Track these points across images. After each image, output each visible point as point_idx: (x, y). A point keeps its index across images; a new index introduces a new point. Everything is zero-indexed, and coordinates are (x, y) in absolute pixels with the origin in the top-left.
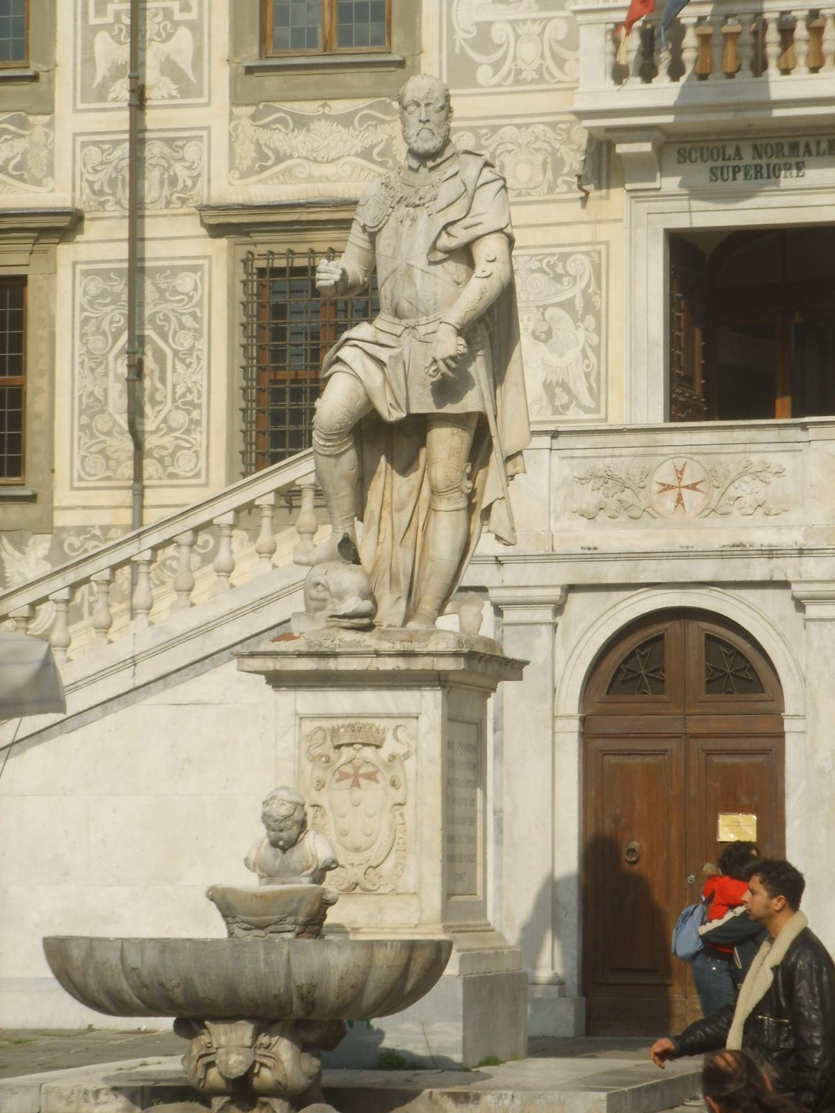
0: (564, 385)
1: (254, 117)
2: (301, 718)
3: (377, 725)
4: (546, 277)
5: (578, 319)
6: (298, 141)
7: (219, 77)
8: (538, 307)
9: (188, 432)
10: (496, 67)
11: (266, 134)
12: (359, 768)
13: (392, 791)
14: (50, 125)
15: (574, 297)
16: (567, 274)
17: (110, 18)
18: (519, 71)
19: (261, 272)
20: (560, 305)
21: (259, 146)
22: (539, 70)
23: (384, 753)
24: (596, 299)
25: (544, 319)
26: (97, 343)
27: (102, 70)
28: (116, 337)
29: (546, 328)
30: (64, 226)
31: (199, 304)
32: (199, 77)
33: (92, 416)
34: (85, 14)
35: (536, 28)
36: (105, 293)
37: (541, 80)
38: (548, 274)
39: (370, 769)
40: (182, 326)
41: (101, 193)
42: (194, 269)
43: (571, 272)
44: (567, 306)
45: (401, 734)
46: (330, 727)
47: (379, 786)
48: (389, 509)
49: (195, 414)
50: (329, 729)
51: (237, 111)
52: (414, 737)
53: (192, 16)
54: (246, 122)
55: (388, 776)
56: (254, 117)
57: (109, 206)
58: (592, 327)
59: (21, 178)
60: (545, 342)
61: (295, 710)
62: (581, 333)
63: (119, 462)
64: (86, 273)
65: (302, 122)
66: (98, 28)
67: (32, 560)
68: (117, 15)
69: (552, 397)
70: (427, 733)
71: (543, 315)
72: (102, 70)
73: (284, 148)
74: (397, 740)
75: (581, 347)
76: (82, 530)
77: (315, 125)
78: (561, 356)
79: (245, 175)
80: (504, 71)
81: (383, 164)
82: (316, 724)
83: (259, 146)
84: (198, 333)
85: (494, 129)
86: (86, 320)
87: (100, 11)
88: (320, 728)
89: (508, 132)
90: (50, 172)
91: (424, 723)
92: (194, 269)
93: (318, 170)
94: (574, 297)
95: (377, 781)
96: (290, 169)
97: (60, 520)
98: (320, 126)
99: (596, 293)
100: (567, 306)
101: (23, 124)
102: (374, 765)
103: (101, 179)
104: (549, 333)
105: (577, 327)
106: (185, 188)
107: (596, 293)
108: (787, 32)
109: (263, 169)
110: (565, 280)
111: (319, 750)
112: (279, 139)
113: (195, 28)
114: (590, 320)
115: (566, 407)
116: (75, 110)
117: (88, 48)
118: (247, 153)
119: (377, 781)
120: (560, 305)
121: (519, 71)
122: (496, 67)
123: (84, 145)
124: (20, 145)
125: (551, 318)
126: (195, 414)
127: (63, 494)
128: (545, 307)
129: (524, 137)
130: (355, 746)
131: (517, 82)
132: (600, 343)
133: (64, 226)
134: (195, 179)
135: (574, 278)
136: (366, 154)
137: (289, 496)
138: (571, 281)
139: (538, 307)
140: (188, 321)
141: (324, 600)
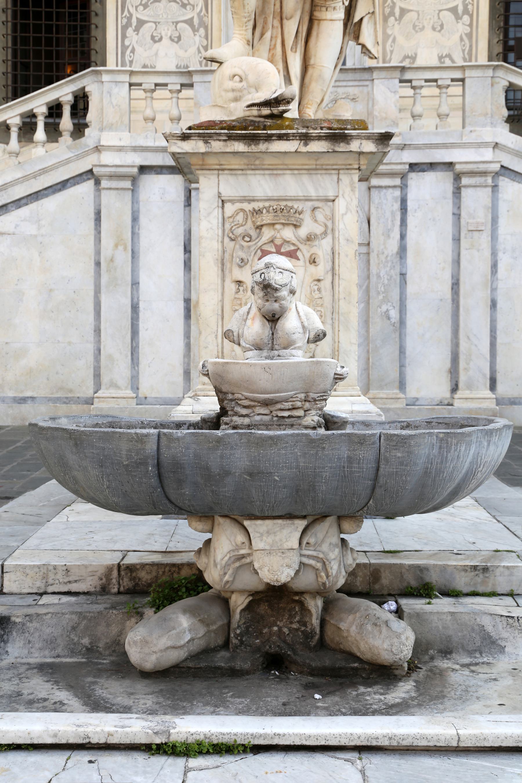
2: (222, 201)
3: (296, 206)
4: (177, 5)
5: (195, 30)
8: (173, 23)
12: (281, 245)
13: (312, 268)
15: (193, 18)
16: (189, 4)
20: (185, 22)
23: (303, 232)
24: (205, 19)
25: (176, 30)
29: (177, 35)
38: (178, 3)
39: (292, 248)
43: (192, 2)
44: (190, 22)
45: (320, 216)
46: (251, 209)
47: (301, 263)
48: (279, 18)
50: (250, 211)
52: (332, 218)
55: (307, 256)
58: (203, 35)
60: (177, 42)
61: (219, 193)
62: (197, 38)
70: (346, 214)
71: (176, 27)
74: (316, 221)
75: (197, 46)
78: (186, 51)
82: (238, 205)
88: (242, 210)
91: (341, 205)
94: (193, 18)
95: (298, 259)
99: (205, 16)
100: (190, 22)
102: (294, 244)
104: (179, 38)
105: (195, 35)
107: (205, 16)
110: (188, 7)
111: (240, 231)
119: (298, 259)
120: (185, 22)
125: (180, 29)
128: (177, 23)
130: (277, 227)
132: (207, 45)
135: (193, 6)
138: (191, 7)
139: (173, 23)
141: (240, 90)
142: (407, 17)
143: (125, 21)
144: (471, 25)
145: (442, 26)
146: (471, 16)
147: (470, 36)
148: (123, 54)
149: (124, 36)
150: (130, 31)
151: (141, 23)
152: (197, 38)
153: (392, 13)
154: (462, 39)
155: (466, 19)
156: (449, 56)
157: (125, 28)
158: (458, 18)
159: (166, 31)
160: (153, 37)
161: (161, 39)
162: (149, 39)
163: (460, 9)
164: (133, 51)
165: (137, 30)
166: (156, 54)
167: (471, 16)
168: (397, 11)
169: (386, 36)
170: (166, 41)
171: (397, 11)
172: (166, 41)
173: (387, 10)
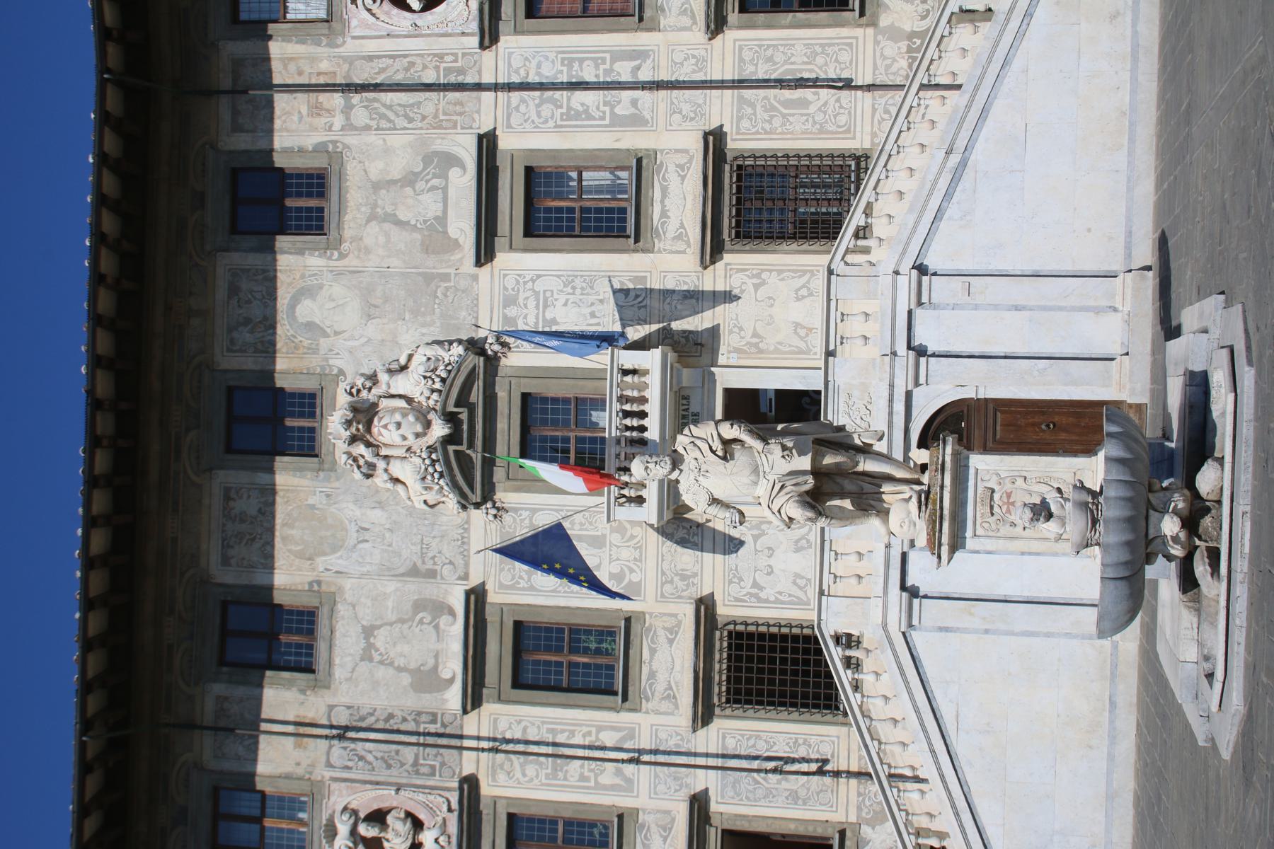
0: (797, 542)
1: (648, 700)
5: (763, 534)
6: (662, 677)
7: (625, 718)
9: (810, 746)
10: (632, 571)
11: (656, 694)
14: (644, 811)
17: (592, 775)
18: (635, 559)
19: (728, 701)
21: (663, 699)
22: (636, 549)
26: (760, 793)
27: (618, 781)
28: (757, 782)
30: (699, 805)
31: (742, 736)
32: (625, 728)
33: (798, 798)
34: (588, 788)
35: (614, 549)
36: (734, 787)
37: (640, 547)
40: (754, 746)
41: (681, 786)
42: (724, 738)
49: (801, 741)
51: (644, 709)
53: (594, 730)
54: (650, 705)
56: (648, 700)
57: (689, 781)
59: (671, 829)
62: (771, 532)
63: (824, 785)
64: (723, 797)
65: (652, 675)
66: (596, 782)
67: (874, 836)
68: (591, 770)
69: (802, 549)
72: (618, 781)
73: (665, 685)
76: (859, 808)
77: (654, 668)
79: (677, 707)
80: (635, 567)
81: (677, 633)
83: (663, 699)
84: (758, 737)
85: (663, 573)
86: (747, 798)
87: (586, 779)
89: (666, 566)
90: (668, 812)
92: (724, 738)
93: (677, 667)
96: (676, 683)
97: (853, 818)
98: (655, 666)
101: (643, 826)
103: (674, 786)
104: (769, 549)
106: (682, 740)
108: (627, 414)
109: (674, 697)
112: (660, 687)
113: (600, 729)
114: (764, 527)
115: (808, 541)
116: (637, 796)
117: (605, 787)
118: (665, 706)
121: (635, 559)
122: (632, 571)
123: (656, 793)
124: (654, 828)
126: (801, 741)
127: (838, 817)
129: (668, 557)
131: (640, 561)
133: (699, 805)
134: (678, 734)
136: (671, 642)
137: (848, 662)
140: (751, 742)
142: (760, 331)
143: (753, 599)
144: (770, 271)
145: (770, 298)
146: (763, 271)
147: (780, 272)
148: (782, 603)
149: (767, 601)
150: (763, 595)
151: (755, 584)
152: (771, 532)
153: (756, 345)
154: (783, 279)
155: (764, 275)
156: (797, 291)
157: (759, 600)
158: (763, 283)
159: (763, 561)
160: (769, 574)
161: (770, 566)
162: (770, 578)
163: (756, 281)
164: (780, 593)
165: (761, 588)
166: (784, 571)
167: (763, 271)
168: (755, 340)
169: (777, 351)
170: (772, 562)
171: (755, 340)
172: (772, 562)
173: (753, 350)
